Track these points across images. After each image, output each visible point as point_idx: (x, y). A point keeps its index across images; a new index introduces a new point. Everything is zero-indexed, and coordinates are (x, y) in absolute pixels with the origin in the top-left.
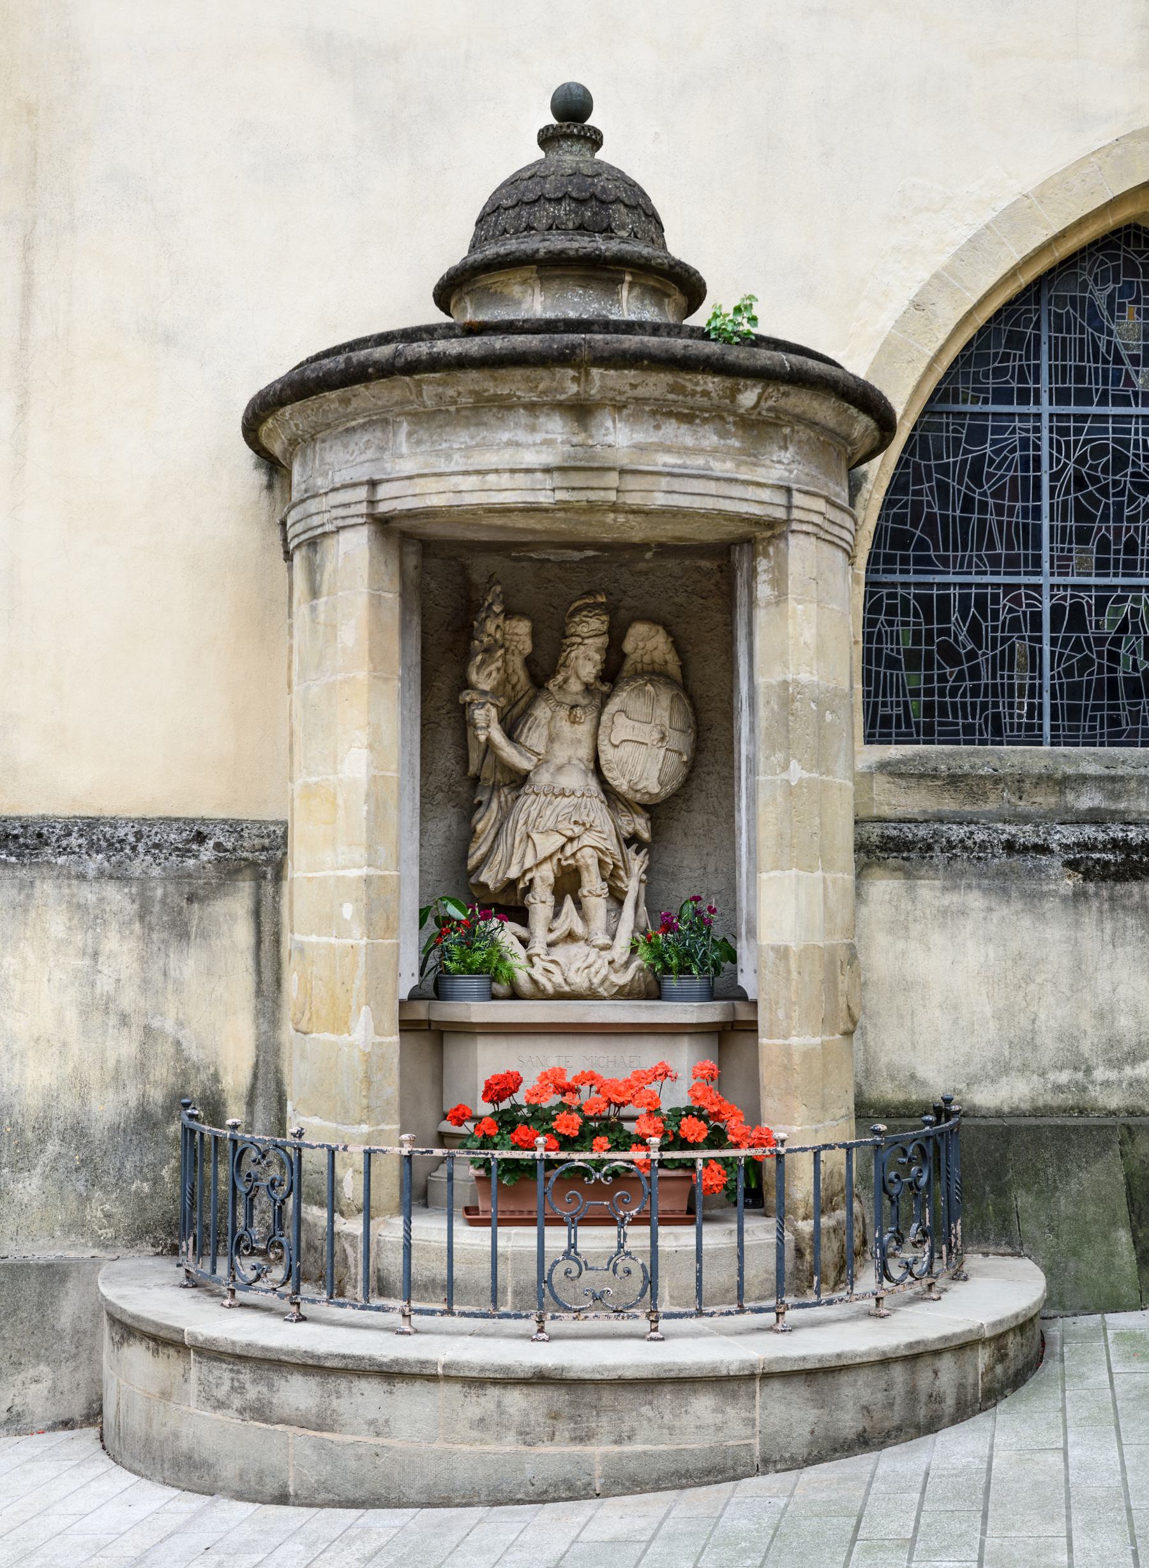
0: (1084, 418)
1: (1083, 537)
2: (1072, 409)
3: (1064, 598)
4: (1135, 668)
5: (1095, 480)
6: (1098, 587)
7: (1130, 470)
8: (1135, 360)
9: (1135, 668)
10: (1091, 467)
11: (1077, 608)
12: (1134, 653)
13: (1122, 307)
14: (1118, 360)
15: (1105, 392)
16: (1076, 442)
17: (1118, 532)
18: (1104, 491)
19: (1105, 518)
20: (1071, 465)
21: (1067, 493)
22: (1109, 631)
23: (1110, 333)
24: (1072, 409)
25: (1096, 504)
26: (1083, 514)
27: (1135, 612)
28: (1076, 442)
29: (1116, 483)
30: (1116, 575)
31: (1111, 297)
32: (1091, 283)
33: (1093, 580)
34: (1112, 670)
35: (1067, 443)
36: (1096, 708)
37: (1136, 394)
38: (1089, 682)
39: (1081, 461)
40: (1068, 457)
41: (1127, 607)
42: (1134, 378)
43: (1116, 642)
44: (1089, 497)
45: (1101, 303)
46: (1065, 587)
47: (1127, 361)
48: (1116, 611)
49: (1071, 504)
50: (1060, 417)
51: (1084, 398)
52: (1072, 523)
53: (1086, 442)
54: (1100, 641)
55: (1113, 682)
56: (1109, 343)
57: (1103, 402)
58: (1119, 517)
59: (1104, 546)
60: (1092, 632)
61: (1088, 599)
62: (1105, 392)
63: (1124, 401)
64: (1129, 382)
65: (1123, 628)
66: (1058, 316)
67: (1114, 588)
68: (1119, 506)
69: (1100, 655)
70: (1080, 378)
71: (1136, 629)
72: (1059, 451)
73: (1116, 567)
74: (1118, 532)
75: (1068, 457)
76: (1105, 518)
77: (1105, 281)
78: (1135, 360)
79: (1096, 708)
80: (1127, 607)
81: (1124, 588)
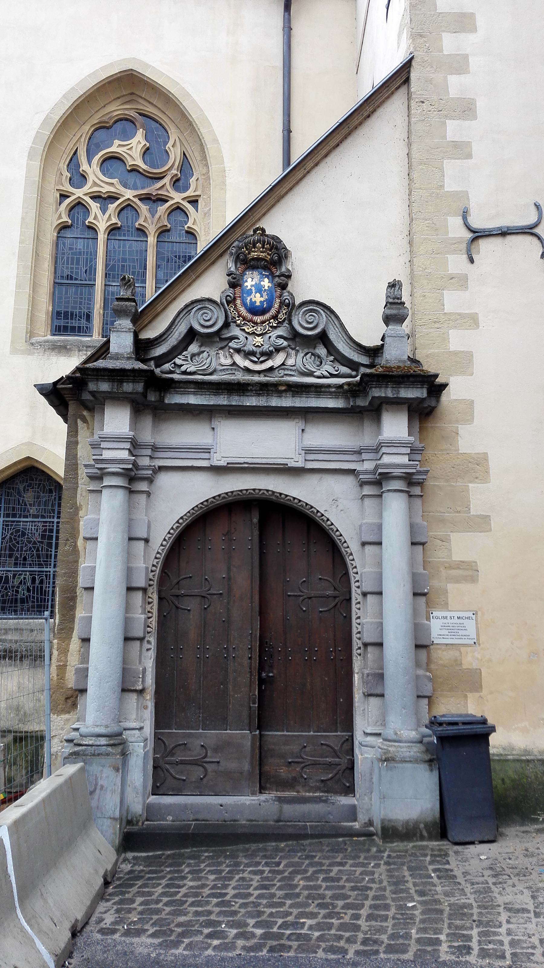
0: (14, 521)
1: (10, 556)
2: (11, 519)
3: (3, 574)
4: (24, 595)
5: (15, 539)
6: (14, 571)
7: (26, 537)
8: (30, 505)
9: (24, 595)
10: (15, 536)
11: (7, 577)
12: (23, 590)
13: (28, 490)
14: (26, 505)
15: (21, 514)
16: (11, 529)
17: (21, 556)
18: (18, 543)
19: (18, 550)
20: (9, 535)
21: (7, 543)
22: (16, 583)
23: (24, 497)
24: (11, 519)
25: (15, 546)
26: (11, 549)
27: (25, 578)
28: (11, 529)
29: (22, 541)
30: (20, 567)
31: (24, 487)
32: (19, 484)
33: (13, 569)
34: (16, 595)
35: (8, 529)
36: (10, 607)
37: (30, 515)
38: (9, 599)
39: (12, 534)
40: (8, 533)
41: (22, 577)
42: (30, 509)
43: (18, 587)
44: (13, 545)
45: (21, 488)
46: (4, 571)
47: (28, 505)
48: (19, 578)
49: (8, 546)
50: (7, 521)
51: (14, 516)
52: (7, 552)
53: (14, 528)
54: (13, 587)
55: (16, 599)
56: (23, 500)
57: (20, 517)
58: (22, 550)
59: (16, 559)
60: (11, 584)
61: (10, 575)
62: (21, 514)
63: (26, 517)
64: (28, 511)
65: (21, 583)
66: (8, 492)
67: (19, 571)
68: (22, 547)
69: (13, 591)
70: (14, 510)
71: (25, 583)
72: (5, 531)
73: (20, 565)
74: (21, 556)
75: (8, 533)
76: (18, 550)
77: (23, 482)
78: (30, 505)
79: (10, 607)
80: (22, 577)
81: (22, 571)
